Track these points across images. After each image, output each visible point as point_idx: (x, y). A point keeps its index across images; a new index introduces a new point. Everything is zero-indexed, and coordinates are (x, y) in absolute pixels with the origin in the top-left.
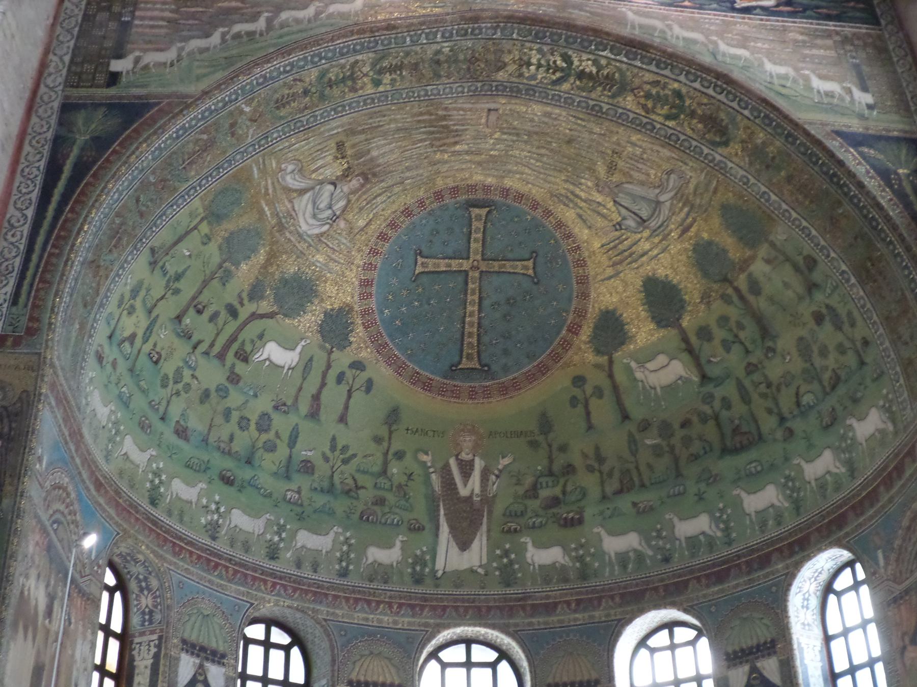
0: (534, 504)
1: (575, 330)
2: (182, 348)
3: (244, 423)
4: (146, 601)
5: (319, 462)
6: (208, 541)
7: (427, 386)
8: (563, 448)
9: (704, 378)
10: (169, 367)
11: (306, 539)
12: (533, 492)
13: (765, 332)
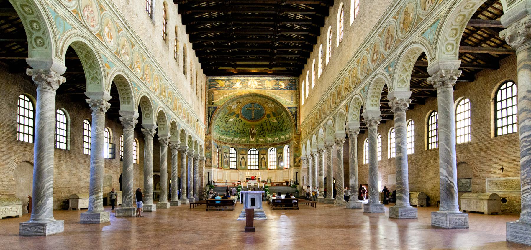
0: (260, 134)
1: (265, 115)
2: (221, 123)
3: (228, 128)
4: (220, 149)
5: (236, 130)
6: (225, 141)
7: (248, 121)
8: (264, 128)
9: (278, 123)
10: (220, 126)
11: (235, 139)
12: (260, 132)
13: (284, 120)
